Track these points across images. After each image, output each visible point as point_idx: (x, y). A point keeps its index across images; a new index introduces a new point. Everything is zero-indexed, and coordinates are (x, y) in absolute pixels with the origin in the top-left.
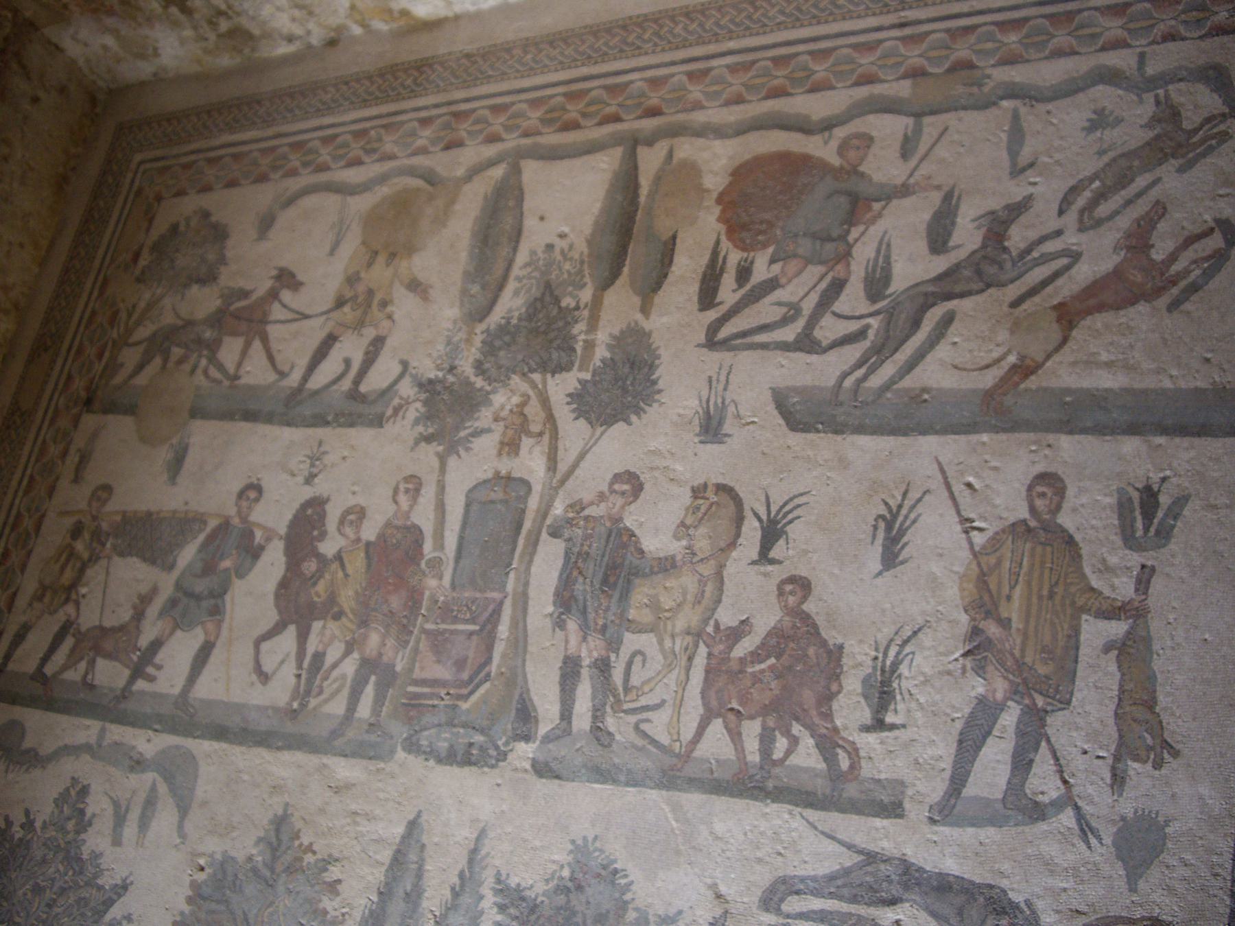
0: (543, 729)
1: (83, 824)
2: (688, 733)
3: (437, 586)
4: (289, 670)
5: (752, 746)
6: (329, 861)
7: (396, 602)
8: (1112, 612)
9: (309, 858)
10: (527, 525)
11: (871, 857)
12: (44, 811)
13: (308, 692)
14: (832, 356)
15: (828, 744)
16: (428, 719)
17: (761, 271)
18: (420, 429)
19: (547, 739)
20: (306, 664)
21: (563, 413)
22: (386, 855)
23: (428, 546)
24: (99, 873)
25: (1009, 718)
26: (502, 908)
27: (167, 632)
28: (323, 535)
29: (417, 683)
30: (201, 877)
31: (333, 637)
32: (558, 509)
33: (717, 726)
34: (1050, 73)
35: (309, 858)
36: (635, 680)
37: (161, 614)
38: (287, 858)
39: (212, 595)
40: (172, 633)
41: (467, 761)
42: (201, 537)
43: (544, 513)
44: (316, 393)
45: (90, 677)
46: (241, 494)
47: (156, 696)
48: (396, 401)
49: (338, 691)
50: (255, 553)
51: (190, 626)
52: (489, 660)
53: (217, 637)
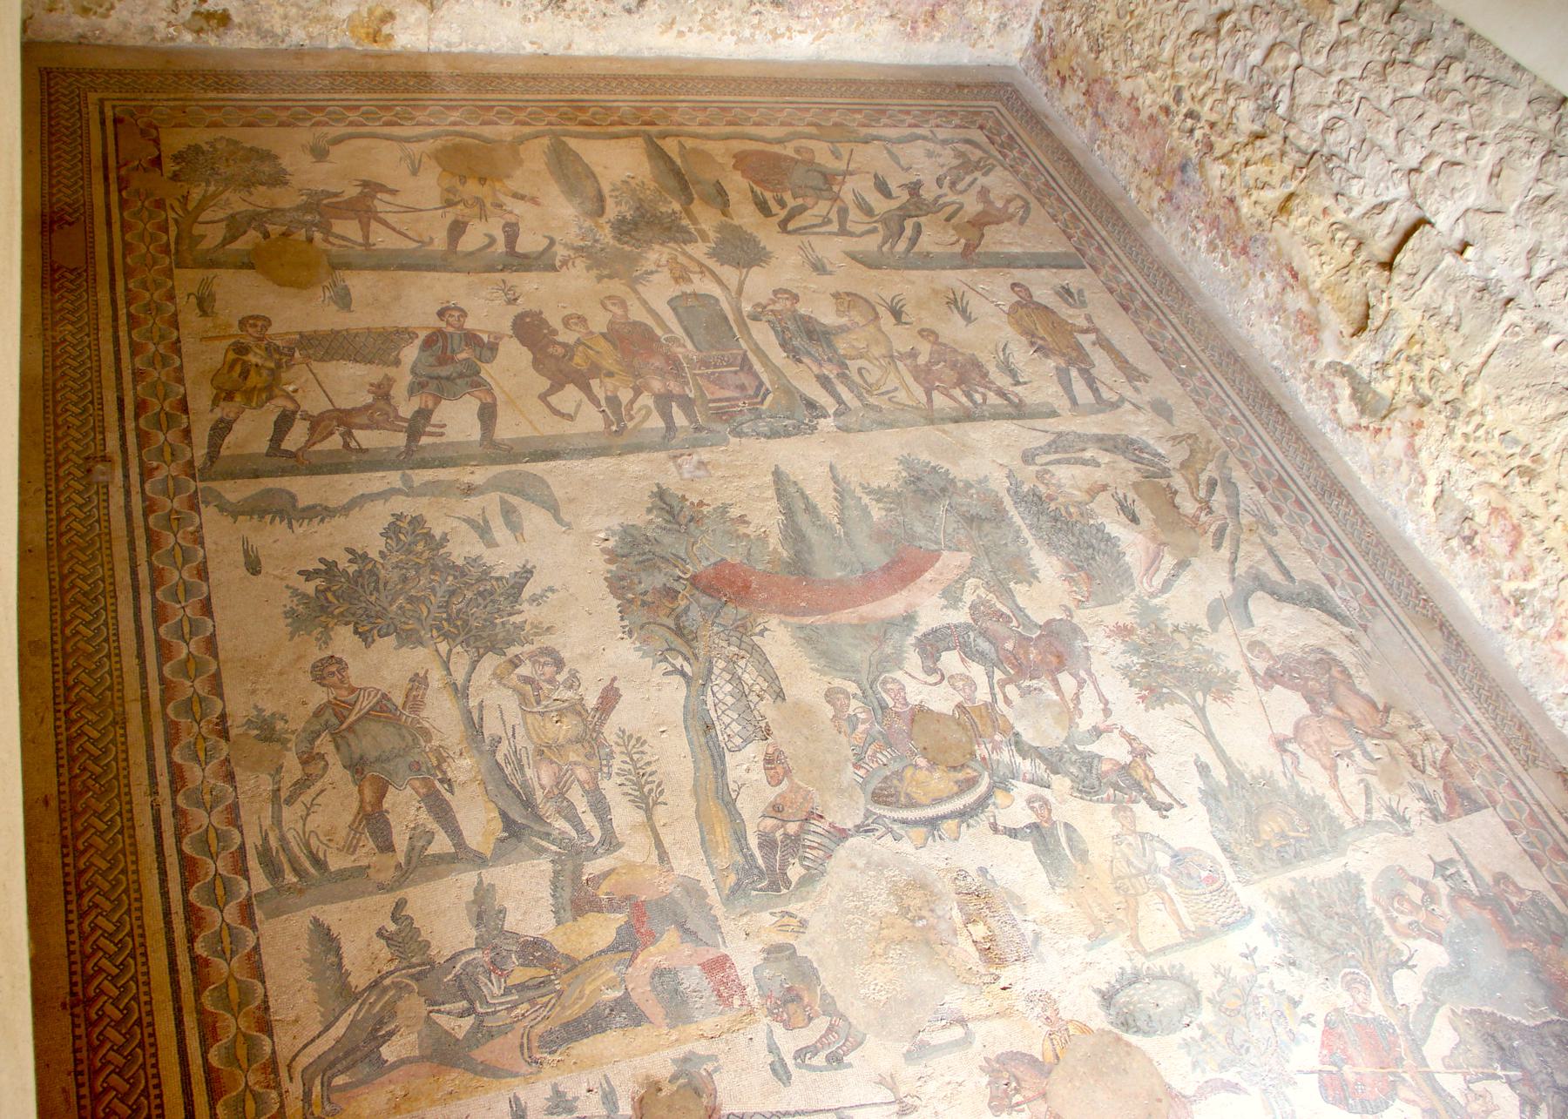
0: (831, 412)
1: (436, 544)
2: (924, 399)
3: (686, 350)
4: (589, 409)
5: (964, 400)
6: (724, 510)
7: (658, 362)
8: (1086, 331)
9: (705, 510)
10: (731, 317)
11: (1060, 435)
12: (375, 546)
13: (620, 420)
14: (867, 238)
15: (1001, 393)
16: (739, 418)
17: (791, 203)
18: (594, 272)
19: (837, 414)
20: (603, 402)
21: (711, 263)
22: (771, 493)
23: (659, 332)
24: (486, 574)
25: (1074, 373)
26: (878, 501)
27: (430, 404)
28: (555, 332)
29: (714, 401)
30: (610, 544)
31: (616, 388)
32: (747, 308)
33: (935, 394)
34: (892, 133)
35: (705, 510)
36: (871, 380)
37: (412, 391)
38: (687, 512)
39: (461, 375)
40: (437, 402)
41: (788, 435)
42: (418, 342)
43: (738, 311)
44: (471, 254)
45: (353, 444)
46: (441, 314)
47: (452, 444)
48: (559, 258)
49: (648, 414)
50: (493, 348)
51: (455, 396)
52: (761, 384)
53: (495, 399)
